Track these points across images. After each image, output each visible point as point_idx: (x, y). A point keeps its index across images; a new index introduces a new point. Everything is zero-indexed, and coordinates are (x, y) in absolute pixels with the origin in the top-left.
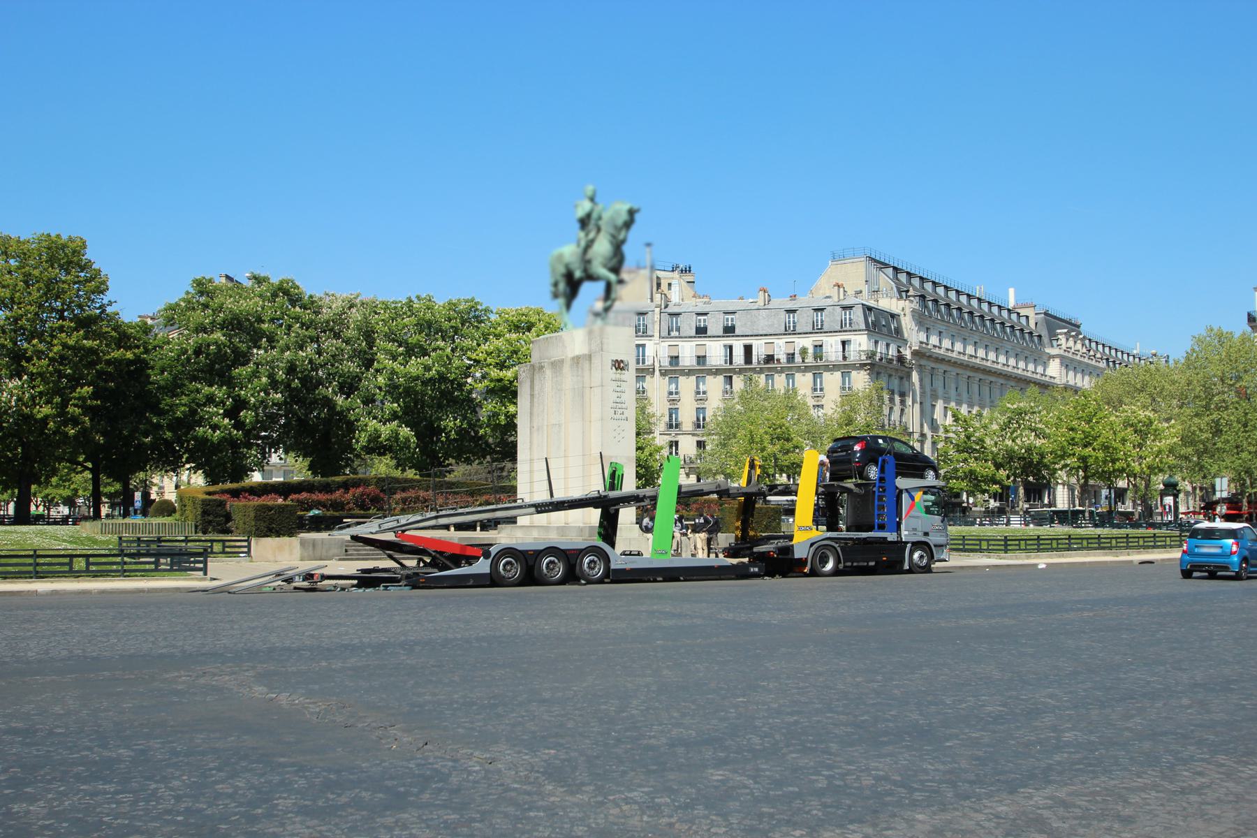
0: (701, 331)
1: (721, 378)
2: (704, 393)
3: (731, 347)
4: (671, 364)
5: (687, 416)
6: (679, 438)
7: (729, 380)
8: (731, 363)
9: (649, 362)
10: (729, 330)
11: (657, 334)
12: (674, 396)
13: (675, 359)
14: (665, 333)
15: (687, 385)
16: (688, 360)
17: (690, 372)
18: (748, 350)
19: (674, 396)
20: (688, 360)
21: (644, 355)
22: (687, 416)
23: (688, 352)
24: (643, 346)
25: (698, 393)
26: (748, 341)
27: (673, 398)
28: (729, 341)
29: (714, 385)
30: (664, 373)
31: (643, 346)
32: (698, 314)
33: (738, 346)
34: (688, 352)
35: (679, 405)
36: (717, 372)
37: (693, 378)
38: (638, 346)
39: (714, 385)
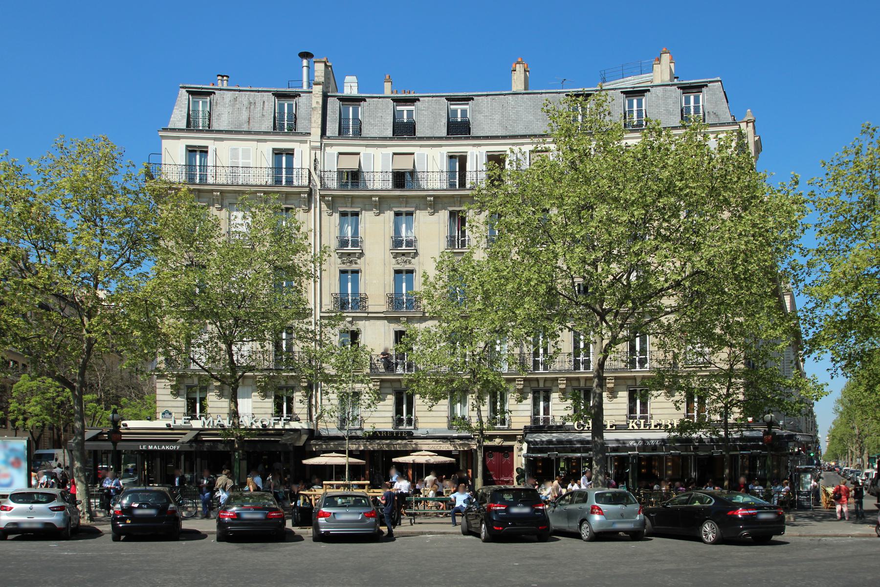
0: (404, 130)
1: (444, 215)
2: (409, 243)
3: (463, 160)
4: (343, 186)
5: (376, 282)
6: (361, 324)
7: (458, 219)
8: (462, 184)
9: (300, 180)
10: (459, 129)
11: (316, 131)
12: (350, 249)
13: (354, 177)
14: (332, 128)
15: (376, 228)
16: (378, 179)
17: (380, 204)
18: (496, 159)
19: (350, 249)
20: (378, 179)
21: (290, 168)
22: (376, 282)
23: (378, 163)
24: (290, 153)
25: (397, 243)
26: (496, 148)
27: (350, 250)
28: (458, 147)
29: (430, 230)
30: (333, 203)
31: (290, 153)
32: (398, 101)
33: (476, 156)
34: (378, 163)
35: (361, 264)
36: (435, 203)
37: (389, 215)
38: (277, 153)
39: (430, 230)
